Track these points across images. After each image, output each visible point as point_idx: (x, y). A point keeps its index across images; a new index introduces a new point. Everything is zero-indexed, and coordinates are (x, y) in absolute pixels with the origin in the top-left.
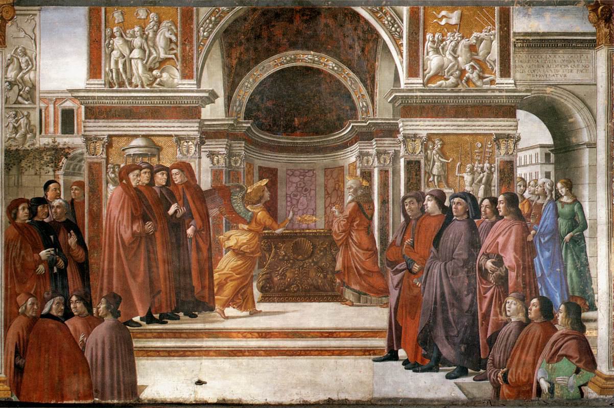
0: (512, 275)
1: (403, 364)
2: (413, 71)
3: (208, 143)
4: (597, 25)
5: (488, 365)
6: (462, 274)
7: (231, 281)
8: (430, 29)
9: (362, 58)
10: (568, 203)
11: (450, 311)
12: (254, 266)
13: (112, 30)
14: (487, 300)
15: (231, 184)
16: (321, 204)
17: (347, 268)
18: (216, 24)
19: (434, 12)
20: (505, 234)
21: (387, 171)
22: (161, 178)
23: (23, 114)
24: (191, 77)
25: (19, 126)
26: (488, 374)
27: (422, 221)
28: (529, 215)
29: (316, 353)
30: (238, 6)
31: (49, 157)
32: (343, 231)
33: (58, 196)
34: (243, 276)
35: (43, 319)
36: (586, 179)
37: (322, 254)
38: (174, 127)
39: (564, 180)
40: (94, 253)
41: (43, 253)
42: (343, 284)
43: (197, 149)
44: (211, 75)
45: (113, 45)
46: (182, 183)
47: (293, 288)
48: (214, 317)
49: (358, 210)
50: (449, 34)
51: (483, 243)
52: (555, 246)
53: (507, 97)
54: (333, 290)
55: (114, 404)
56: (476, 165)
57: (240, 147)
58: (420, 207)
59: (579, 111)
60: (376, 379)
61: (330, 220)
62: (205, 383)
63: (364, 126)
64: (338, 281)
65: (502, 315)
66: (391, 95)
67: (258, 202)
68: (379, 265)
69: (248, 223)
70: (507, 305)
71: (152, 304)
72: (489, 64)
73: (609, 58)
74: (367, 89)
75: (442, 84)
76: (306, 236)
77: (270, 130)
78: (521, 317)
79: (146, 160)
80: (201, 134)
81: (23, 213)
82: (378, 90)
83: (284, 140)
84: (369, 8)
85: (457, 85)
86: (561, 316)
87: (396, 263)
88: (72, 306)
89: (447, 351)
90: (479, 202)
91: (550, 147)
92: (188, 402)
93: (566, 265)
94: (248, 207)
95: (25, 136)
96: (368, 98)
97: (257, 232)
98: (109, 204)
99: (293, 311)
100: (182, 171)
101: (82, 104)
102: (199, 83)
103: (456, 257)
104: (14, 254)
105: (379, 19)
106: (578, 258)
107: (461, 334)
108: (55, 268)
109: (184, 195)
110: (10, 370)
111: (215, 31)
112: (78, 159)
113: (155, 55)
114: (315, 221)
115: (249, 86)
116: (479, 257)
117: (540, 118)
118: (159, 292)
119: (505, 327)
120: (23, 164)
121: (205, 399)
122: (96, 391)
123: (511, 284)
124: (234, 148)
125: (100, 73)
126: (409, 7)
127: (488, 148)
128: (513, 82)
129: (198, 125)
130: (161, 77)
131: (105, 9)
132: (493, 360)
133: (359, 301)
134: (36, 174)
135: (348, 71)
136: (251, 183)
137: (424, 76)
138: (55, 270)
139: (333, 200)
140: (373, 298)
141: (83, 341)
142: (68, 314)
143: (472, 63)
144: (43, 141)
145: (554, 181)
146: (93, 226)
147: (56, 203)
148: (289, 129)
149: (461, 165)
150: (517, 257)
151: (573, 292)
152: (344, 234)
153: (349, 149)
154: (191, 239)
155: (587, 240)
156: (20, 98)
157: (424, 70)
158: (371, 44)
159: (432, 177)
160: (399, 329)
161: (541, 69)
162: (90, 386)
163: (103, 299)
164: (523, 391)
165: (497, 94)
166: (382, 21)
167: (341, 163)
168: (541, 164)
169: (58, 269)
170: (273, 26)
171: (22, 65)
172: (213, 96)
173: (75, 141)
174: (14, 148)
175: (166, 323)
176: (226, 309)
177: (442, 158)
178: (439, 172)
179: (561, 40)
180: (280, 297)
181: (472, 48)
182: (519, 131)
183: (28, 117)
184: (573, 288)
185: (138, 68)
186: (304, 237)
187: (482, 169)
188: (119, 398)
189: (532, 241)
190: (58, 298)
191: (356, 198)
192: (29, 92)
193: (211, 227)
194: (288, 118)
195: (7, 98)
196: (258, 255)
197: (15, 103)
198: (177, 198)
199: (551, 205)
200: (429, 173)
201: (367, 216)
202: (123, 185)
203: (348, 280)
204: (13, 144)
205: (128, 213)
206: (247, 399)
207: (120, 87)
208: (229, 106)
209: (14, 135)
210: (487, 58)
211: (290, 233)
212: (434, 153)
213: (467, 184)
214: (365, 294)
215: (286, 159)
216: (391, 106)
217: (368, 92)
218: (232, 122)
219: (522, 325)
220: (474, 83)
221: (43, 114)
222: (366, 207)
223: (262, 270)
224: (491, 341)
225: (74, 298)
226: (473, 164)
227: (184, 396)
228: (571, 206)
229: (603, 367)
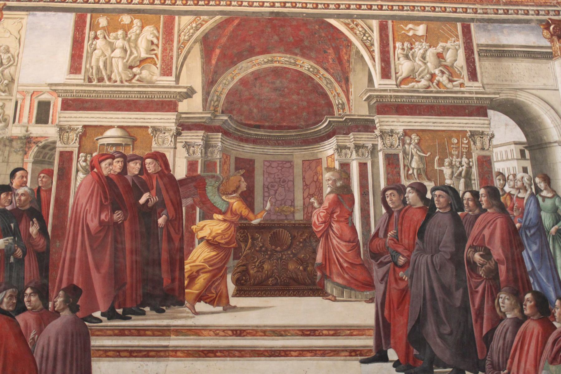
0: (503, 268)
1: (394, 366)
2: (386, 74)
5: (486, 367)
7: (203, 273)
10: (548, 198)
12: (230, 256)
13: (96, 33)
14: (479, 295)
19: (402, 25)
21: (366, 164)
22: (134, 168)
24: (170, 74)
29: (296, 354)
30: (218, 15)
32: (324, 222)
33: (24, 184)
34: (217, 269)
43: (173, 140)
45: (95, 45)
50: (417, 43)
51: (469, 235)
53: (477, 98)
54: (314, 284)
56: (454, 160)
57: (217, 138)
58: (402, 199)
61: (310, 211)
63: (341, 122)
66: (365, 94)
67: (235, 192)
68: (362, 257)
70: (500, 300)
71: (116, 297)
76: (285, 227)
80: (178, 126)
82: (353, 89)
87: (381, 255)
88: (26, 299)
90: (461, 196)
94: (223, 197)
96: (343, 95)
97: (232, 222)
101: (59, 96)
113: (136, 54)
117: (511, 118)
124: (211, 140)
126: (377, 21)
127: (464, 144)
128: (481, 85)
130: (141, 73)
137: (397, 79)
138: (12, 260)
141: (33, 339)
142: (21, 308)
143: (441, 68)
144: (16, 131)
145: (532, 176)
147: (21, 191)
153: (326, 142)
154: (162, 228)
163: (61, 293)
167: (320, 156)
169: (15, 258)
175: (130, 318)
176: (198, 303)
177: (420, 152)
178: (418, 165)
179: (520, 51)
181: (440, 56)
182: (492, 130)
185: (118, 66)
187: (460, 163)
190: (11, 290)
192: (7, 85)
196: (234, 245)
200: (408, 167)
212: (411, 148)
216: (366, 104)
218: (209, 115)
219: (518, 322)
224: (488, 339)
226: (451, 158)
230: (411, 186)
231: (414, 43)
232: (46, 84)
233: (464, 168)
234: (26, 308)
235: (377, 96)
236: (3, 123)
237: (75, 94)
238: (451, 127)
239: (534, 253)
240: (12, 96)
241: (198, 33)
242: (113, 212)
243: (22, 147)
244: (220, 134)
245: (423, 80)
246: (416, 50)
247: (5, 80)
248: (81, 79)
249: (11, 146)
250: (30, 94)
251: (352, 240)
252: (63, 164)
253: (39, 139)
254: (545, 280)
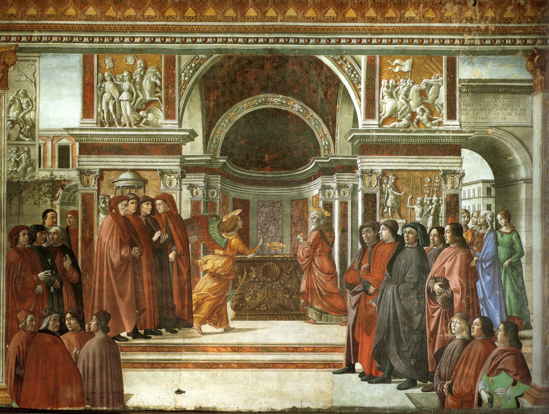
0: (457, 297)
1: (359, 377)
2: (370, 114)
3: (188, 177)
4: (533, 72)
6: (413, 296)
7: (207, 300)
8: (385, 75)
9: (325, 101)
10: (507, 233)
11: (401, 329)
14: (435, 319)
15: (208, 213)
16: (287, 232)
17: (310, 289)
18: (196, 69)
20: (451, 260)
21: (346, 203)
22: (146, 208)
23: (24, 150)
24: (173, 118)
26: (435, 385)
27: (377, 249)
28: (472, 244)
29: (282, 366)
31: (47, 189)
32: (308, 257)
33: (54, 224)
35: (42, 334)
36: (523, 212)
37: (288, 276)
38: (158, 162)
39: (503, 212)
40: (86, 274)
41: (41, 275)
42: (307, 303)
43: (179, 182)
44: (191, 116)
45: (104, 88)
46: (165, 212)
47: (263, 307)
48: (192, 333)
49: (321, 238)
50: (402, 80)
51: (431, 267)
52: (495, 271)
53: (453, 137)
54: (297, 309)
55: (103, 411)
56: (425, 198)
57: (217, 180)
59: (517, 150)
60: (335, 389)
61: (296, 247)
62: (184, 392)
64: (302, 301)
65: (447, 333)
66: (350, 135)
67: (232, 230)
69: (224, 249)
71: (138, 321)
72: (437, 108)
73: (544, 104)
74: (329, 129)
75: (395, 125)
76: (275, 261)
77: (243, 166)
78: (465, 334)
79: (133, 191)
81: (23, 238)
83: (255, 174)
84: (331, 56)
85: (408, 126)
86: (500, 335)
87: (354, 285)
88: (67, 322)
89: (398, 364)
90: (428, 232)
91: (492, 182)
92: (169, 409)
93: (505, 288)
95: (25, 169)
96: (329, 137)
97: (230, 257)
98: (100, 231)
99: (263, 328)
100: (165, 201)
101: (76, 141)
102: (180, 123)
103: (407, 280)
104: (15, 275)
105: (340, 67)
106: (516, 282)
107: (411, 350)
108: (52, 288)
109: (167, 224)
110: (11, 379)
111: (195, 77)
112: (73, 190)
113: (141, 97)
114: (282, 248)
115: (225, 126)
116: (427, 281)
117: (482, 157)
118: (144, 310)
119: (450, 344)
120: (24, 194)
121: (184, 407)
122: (88, 399)
123: (456, 305)
125: (93, 114)
126: (366, 56)
127: (436, 182)
128: (458, 123)
129: (179, 160)
130: (147, 117)
131: (98, 56)
132: (440, 373)
133: (321, 319)
134: (36, 204)
135: (312, 112)
136: (226, 213)
137: (380, 118)
139: (299, 228)
140: (333, 317)
141: (76, 354)
142: (63, 330)
143: (422, 106)
144: (42, 174)
146: (86, 250)
147: (53, 229)
148: (260, 165)
149: (412, 198)
150: (462, 280)
151: (511, 312)
152: (308, 259)
153: (312, 183)
154: (173, 262)
155: (524, 266)
156: (21, 136)
157: (380, 113)
158: (333, 89)
159: (386, 209)
160: (356, 345)
161: (484, 113)
162: (82, 394)
163: (94, 317)
164: (465, 402)
165: (444, 134)
166: (342, 69)
167: (306, 196)
168: (483, 197)
169: (54, 289)
170: (246, 72)
172: (193, 135)
173: (71, 174)
174: (15, 180)
175: (150, 338)
177: (395, 191)
178: (393, 204)
179: (500, 86)
180: (252, 315)
181: (422, 93)
182: (463, 168)
183: (28, 152)
184: (511, 309)
185: (126, 109)
186: (273, 261)
187: (431, 201)
188: (108, 406)
189: (475, 266)
191: (319, 227)
192: (29, 130)
193: (190, 253)
194: (259, 155)
195: (9, 135)
196: (231, 277)
197: (17, 140)
198: (161, 226)
199: (492, 235)
201: (328, 243)
202: (112, 215)
203: (312, 301)
204: (15, 176)
205: (116, 239)
206: (221, 407)
207: (110, 126)
208: (207, 145)
209: (16, 169)
210: (436, 102)
211: (261, 258)
212: (388, 188)
213: (417, 215)
214: (326, 313)
215: (257, 191)
216: (350, 144)
217: (330, 132)
218: (209, 158)
219: (465, 342)
220: (424, 125)
221: (42, 149)
222: (327, 235)
223: (236, 290)
224: (438, 356)
225: (68, 315)
227: (165, 404)
228: (510, 235)
229: (537, 380)
230: (385, 224)
231: (399, 80)
233: (434, 206)
234: (68, 329)
235: (360, 137)
237: (90, 138)
238: (426, 166)
239: (487, 284)
241: (197, 74)
242: (131, 248)
244: (220, 176)
245: (404, 119)
246: (401, 87)
248: (94, 124)
251: (331, 272)
252: (86, 206)
254: (493, 307)
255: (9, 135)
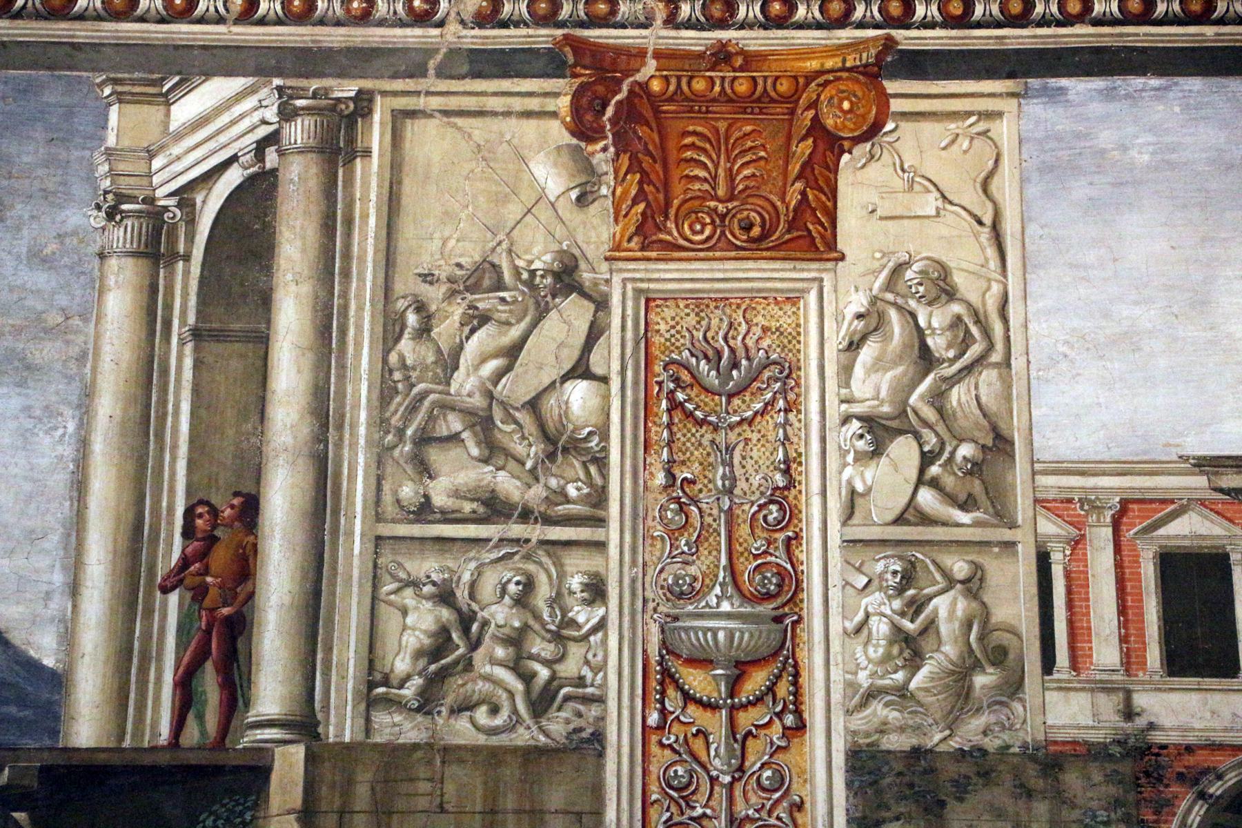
23: (946, 574)
25: (924, 631)
95: (961, 674)
156: (926, 497)
171: (930, 341)
174: (895, 742)
183: (973, 585)
192: (975, 468)
209: (900, 676)
221: (1057, 572)
232: (1183, 458)
236: (991, 670)
240: (1013, 526)
243: (1117, 803)
247: (961, 440)
249: (1060, 797)
250: (1108, 514)
253: (1201, 759)
255: (853, 492)
